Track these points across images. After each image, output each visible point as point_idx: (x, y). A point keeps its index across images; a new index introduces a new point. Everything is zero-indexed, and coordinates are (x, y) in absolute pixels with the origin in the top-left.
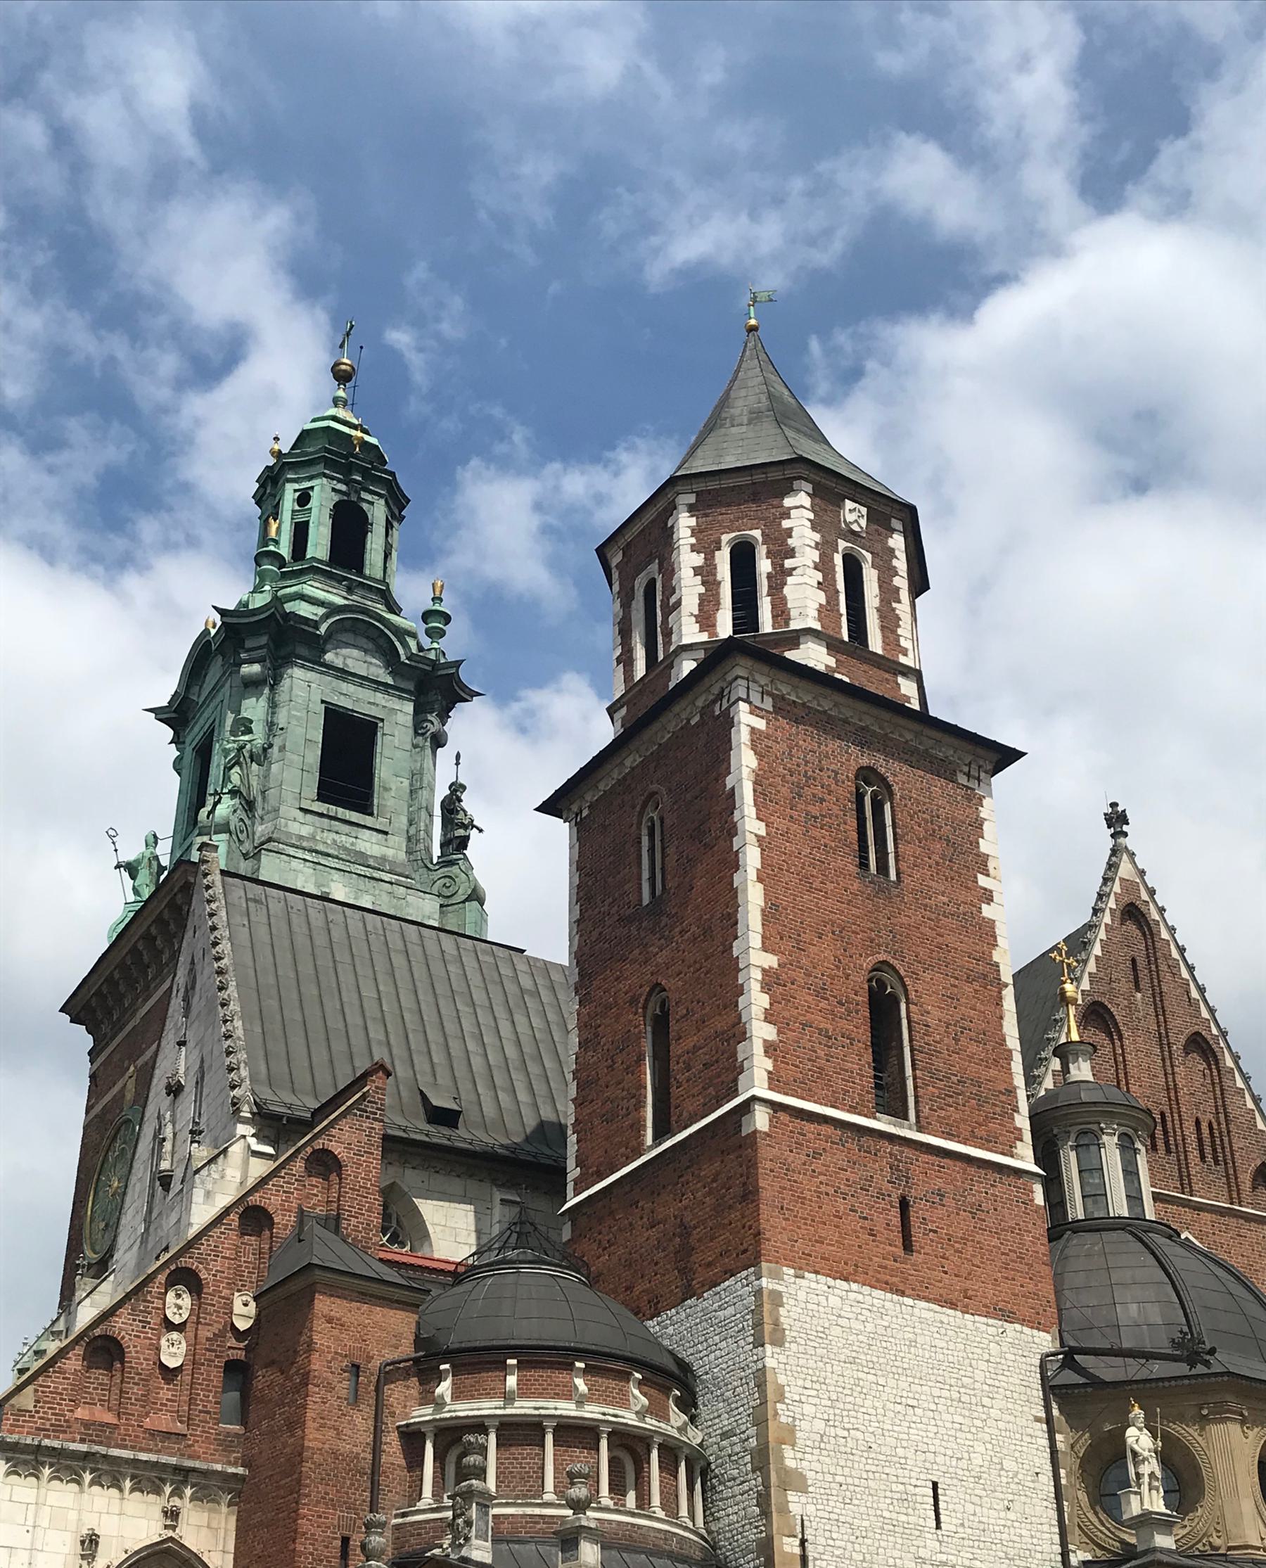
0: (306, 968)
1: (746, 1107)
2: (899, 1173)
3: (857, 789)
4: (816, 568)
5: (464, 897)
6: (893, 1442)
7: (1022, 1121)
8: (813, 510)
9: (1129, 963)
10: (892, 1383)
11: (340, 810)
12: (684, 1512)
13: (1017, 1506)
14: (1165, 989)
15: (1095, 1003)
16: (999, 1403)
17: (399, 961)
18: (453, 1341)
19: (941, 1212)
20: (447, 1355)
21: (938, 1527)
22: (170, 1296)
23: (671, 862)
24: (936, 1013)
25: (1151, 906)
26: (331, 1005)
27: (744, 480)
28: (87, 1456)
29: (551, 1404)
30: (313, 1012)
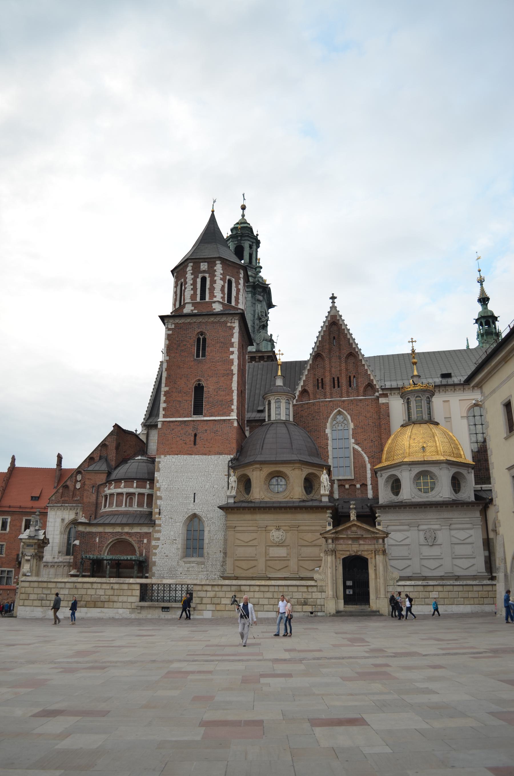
4: (191, 285)
6: (185, 486)
7: (234, 407)
8: (192, 270)
10: (186, 474)
12: (145, 505)
13: (216, 495)
15: (318, 353)
16: (214, 474)
19: (206, 434)
21: (194, 501)
22: (78, 477)
24: (213, 387)
25: (340, 320)
27: (181, 267)
28: (62, 506)
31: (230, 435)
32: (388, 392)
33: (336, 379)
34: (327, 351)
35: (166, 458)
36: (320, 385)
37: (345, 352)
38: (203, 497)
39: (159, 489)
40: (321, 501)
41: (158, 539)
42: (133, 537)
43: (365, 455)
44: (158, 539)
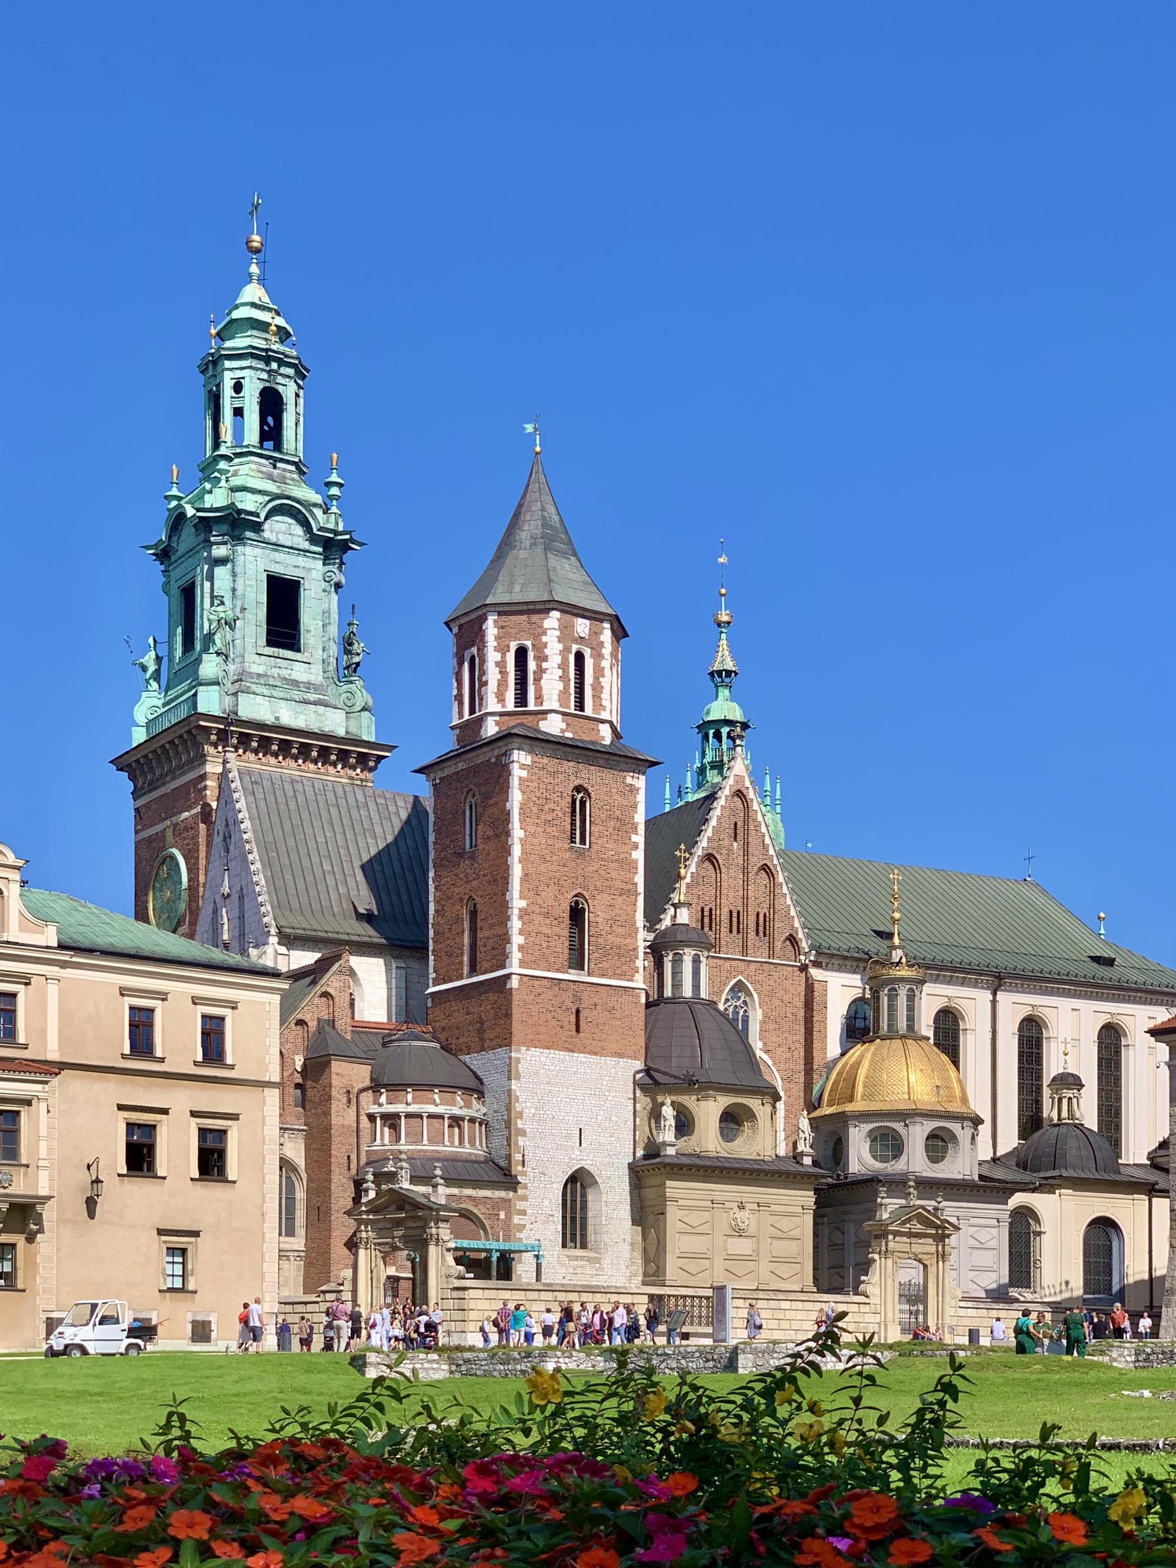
0: (288, 828)
1: (508, 976)
2: (577, 998)
3: (573, 796)
5: (360, 708)
9: (732, 826)
10: (565, 1090)
11: (281, 651)
12: (477, 1143)
14: (750, 840)
16: (611, 1094)
17: (334, 811)
18: (385, 1082)
19: (595, 1012)
20: (384, 1086)
23: (480, 835)
26: (303, 851)
29: (426, 1106)
30: (294, 857)
31: (635, 1019)
32: (824, 960)
33: (735, 915)
34: (724, 852)
35: (530, 1052)
36: (706, 920)
37: (756, 861)
38: (595, 1137)
39: (520, 1115)
40: (802, 1165)
41: (524, 1213)
42: (480, 1206)
43: (777, 1075)
44: (524, 1213)
